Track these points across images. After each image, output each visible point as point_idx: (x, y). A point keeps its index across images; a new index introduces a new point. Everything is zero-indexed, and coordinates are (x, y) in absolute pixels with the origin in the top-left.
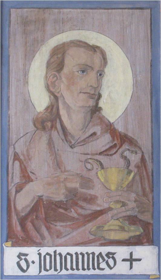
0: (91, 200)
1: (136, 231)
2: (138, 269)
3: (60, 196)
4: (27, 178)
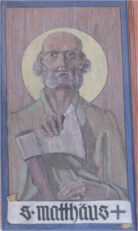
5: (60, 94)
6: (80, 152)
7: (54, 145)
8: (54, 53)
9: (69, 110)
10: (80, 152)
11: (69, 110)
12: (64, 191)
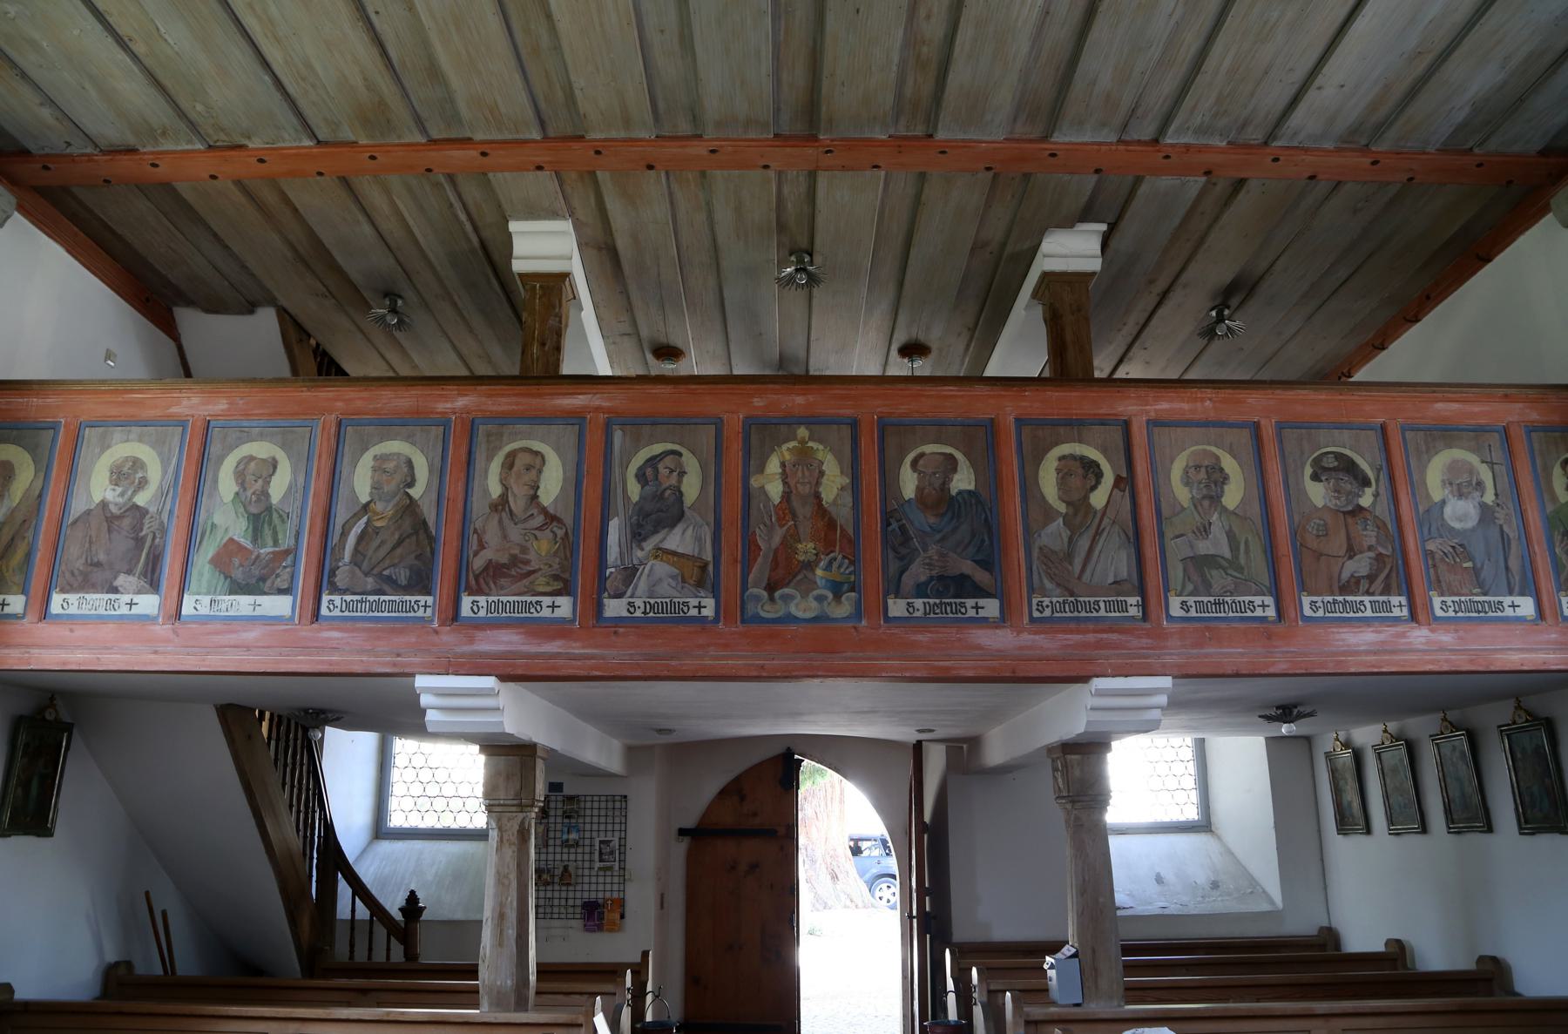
0: (527, 562)
1: (558, 585)
2: (559, 613)
3: (504, 560)
4: (482, 546)
5: (1206, 503)
6: (1227, 554)
7: (1204, 547)
8: (1197, 467)
9: (1215, 517)
10: (1227, 554)
11: (1215, 517)
12: (1216, 587)
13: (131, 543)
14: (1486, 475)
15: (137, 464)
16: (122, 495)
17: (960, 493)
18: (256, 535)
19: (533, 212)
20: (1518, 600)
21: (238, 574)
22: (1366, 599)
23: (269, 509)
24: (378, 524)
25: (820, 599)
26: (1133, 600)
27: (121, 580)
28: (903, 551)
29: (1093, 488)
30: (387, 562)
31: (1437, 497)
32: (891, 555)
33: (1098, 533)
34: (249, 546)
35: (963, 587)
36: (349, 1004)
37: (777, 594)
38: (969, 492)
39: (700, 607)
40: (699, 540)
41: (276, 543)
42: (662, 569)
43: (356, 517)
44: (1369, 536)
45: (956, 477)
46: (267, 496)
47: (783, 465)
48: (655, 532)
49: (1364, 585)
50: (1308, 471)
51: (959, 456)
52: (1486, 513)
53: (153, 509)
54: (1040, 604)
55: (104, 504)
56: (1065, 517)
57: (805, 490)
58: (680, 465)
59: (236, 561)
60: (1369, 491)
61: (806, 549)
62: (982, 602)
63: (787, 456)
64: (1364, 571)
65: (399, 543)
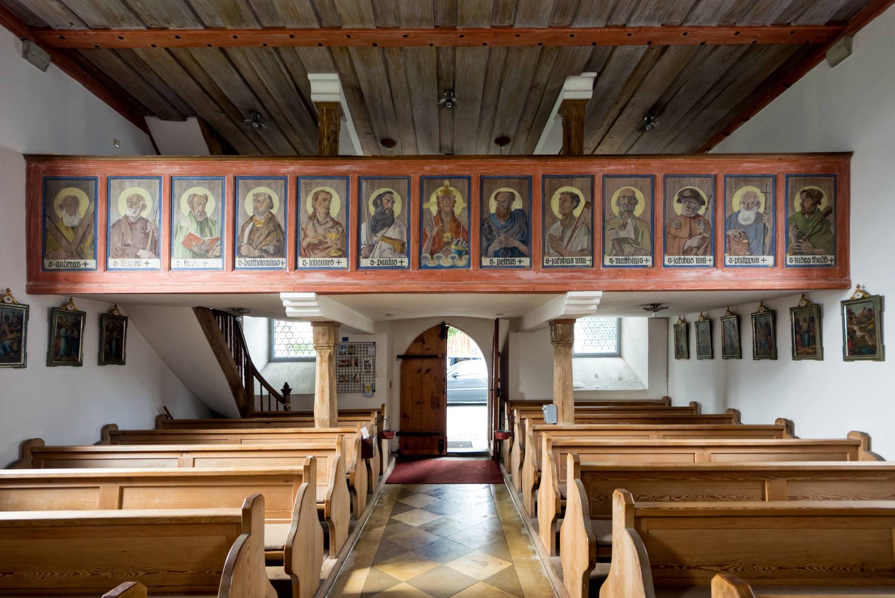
0: (326, 243)
1: (340, 253)
2: (341, 265)
3: (316, 242)
4: (306, 236)
5: (626, 214)
6: (633, 237)
7: (623, 234)
8: (624, 197)
9: (629, 220)
10: (633, 237)
11: (629, 220)
12: (626, 252)
13: (143, 235)
14: (762, 198)
15: (140, 198)
16: (134, 212)
17: (516, 210)
18: (202, 231)
19: (319, 70)
20: (766, 257)
21: (196, 249)
22: (695, 257)
23: (206, 219)
24: (258, 226)
25: (453, 258)
26: (588, 258)
27: (141, 252)
28: (489, 237)
29: (575, 207)
30: (264, 243)
31: (736, 210)
32: (484, 238)
33: (575, 228)
34: (198, 235)
35: (514, 252)
36: (261, 428)
37: (435, 256)
38: (520, 210)
39: (402, 262)
40: (401, 232)
41: (211, 235)
42: (385, 245)
43: (247, 223)
44: (700, 228)
45: (514, 203)
46: (205, 213)
47: (438, 198)
48: (382, 229)
49: (695, 251)
50: (676, 198)
51: (516, 193)
52: (759, 217)
53: (151, 219)
54: (547, 260)
55: (126, 217)
56: (561, 221)
57: (447, 209)
58: (392, 198)
59: (194, 243)
60: (704, 207)
61: (447, 236)
62: (522, 259)
63: (440, 194)
64: (695, 245)
65: (269, 234)
